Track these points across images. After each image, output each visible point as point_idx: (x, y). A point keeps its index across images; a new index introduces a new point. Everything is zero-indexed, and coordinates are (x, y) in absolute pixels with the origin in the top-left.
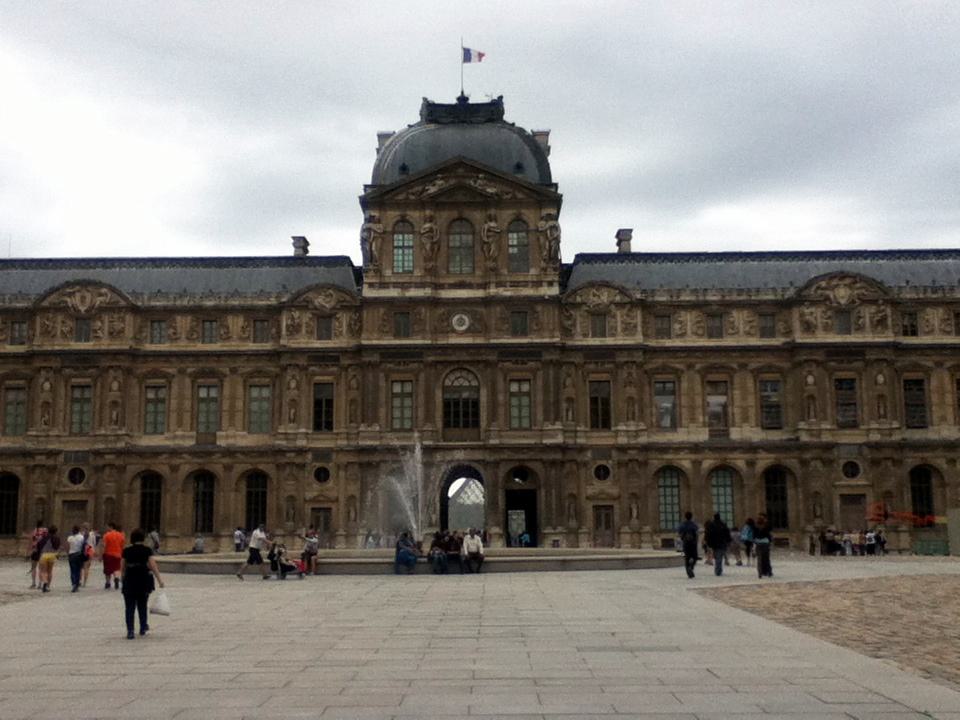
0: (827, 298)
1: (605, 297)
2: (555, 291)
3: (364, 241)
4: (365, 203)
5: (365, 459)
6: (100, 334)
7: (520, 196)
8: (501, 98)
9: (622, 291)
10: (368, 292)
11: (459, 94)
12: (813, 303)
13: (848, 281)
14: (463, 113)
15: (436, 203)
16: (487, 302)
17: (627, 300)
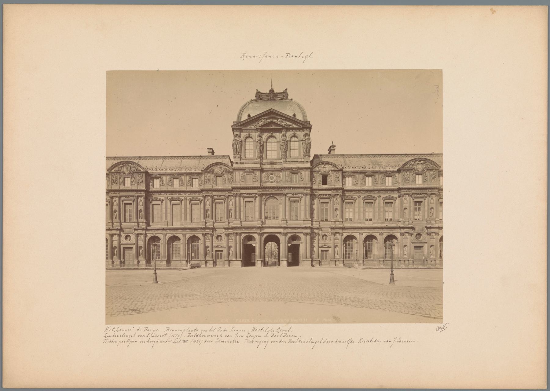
0: (414, 169)
1: (328, 168)
2: (309, 165)
3: (233, 144)
4: (234, 130)
5: (235, 231)
6: (134, 183)
7: (295, 126)
8: (286, 89)
9: (334, 166)
10: (235, 166)
11: (270, 88)
12: (408, 170)
13: (422, 162)
14: (272, 96)
15: (262, 130)
16: (282, 170)
17: (336, 169)
